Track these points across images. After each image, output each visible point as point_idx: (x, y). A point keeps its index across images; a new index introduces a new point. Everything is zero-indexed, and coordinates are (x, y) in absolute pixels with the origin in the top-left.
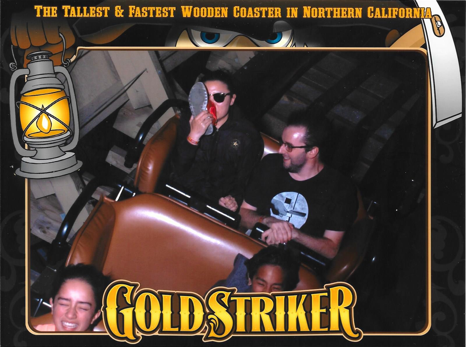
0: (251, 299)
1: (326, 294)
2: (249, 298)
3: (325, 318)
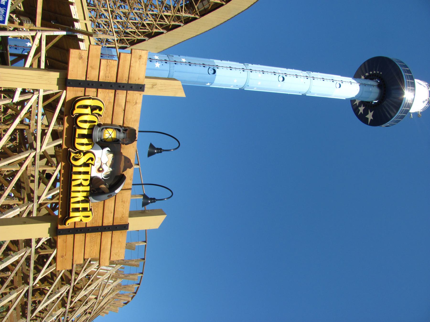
0: (89, 174)
2: (90, 173)
3: (77, 210)
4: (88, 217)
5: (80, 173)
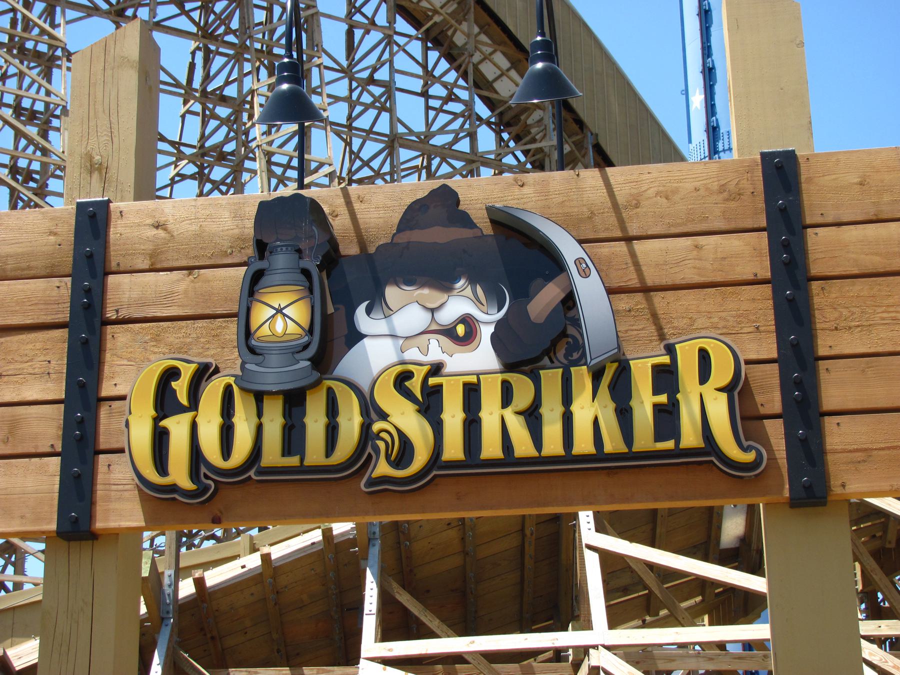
0: (479, 379)
1: (666, 359)
2: (474, 379)
4: (704, 357)
5: (472, 426)
